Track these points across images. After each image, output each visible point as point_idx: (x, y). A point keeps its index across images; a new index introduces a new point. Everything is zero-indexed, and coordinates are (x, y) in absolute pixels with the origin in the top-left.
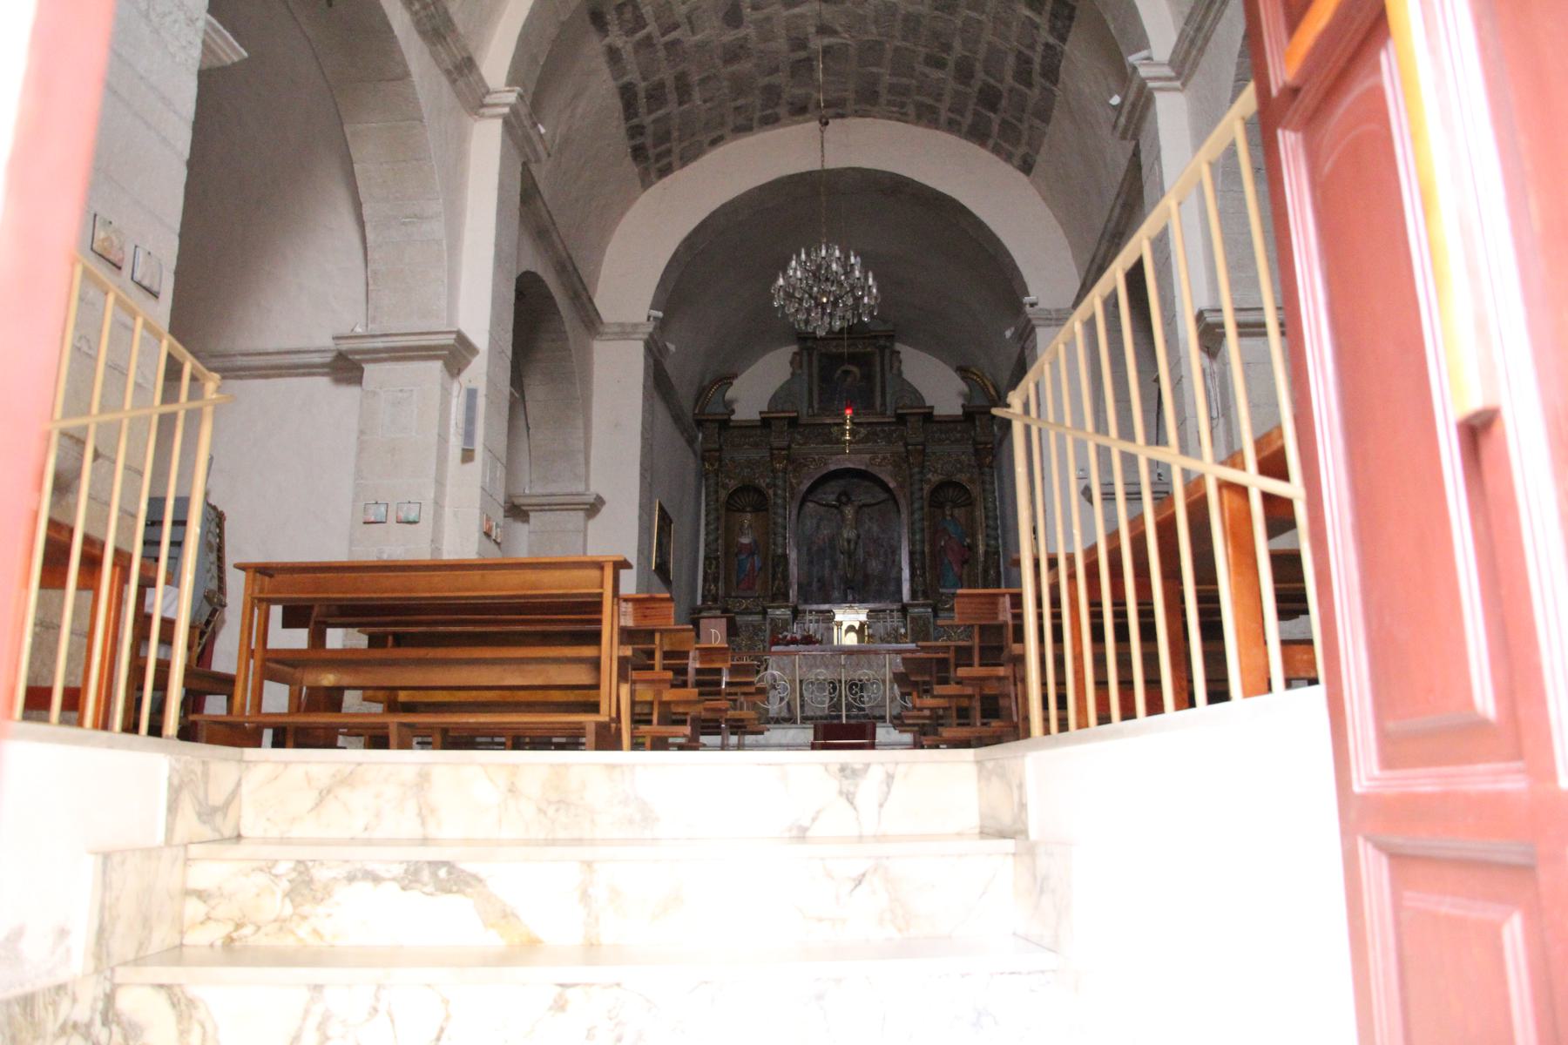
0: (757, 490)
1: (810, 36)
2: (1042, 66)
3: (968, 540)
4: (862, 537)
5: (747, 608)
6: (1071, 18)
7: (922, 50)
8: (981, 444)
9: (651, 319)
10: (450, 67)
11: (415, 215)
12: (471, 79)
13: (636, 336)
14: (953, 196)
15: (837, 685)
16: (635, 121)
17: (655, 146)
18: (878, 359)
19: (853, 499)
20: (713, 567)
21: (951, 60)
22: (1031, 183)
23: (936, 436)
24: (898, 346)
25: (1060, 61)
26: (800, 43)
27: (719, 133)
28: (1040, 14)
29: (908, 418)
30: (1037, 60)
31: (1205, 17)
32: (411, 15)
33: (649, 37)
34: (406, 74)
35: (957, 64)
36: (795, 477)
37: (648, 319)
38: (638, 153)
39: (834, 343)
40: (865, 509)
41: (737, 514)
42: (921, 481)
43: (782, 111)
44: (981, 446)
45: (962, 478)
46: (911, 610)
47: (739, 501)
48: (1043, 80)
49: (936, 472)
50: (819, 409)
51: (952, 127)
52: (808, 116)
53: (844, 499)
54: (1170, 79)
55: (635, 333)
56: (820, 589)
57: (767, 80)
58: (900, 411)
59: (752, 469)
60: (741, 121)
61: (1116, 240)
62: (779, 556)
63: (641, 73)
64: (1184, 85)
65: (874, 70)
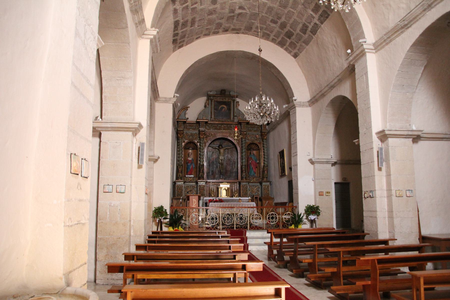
0: (194, 143)
1: (236, 9)
2: (311, 29)
3: (258, 161)
4: (225, 158)
5: (191, 181)
6: (327, 17)
7: (271, 18)
8: (263, 132)
9: (175, 97)
10: (137, 22)
11: (122, 77)
12: (142, 26)
13: (170, 102)
14: (272, 63)
15: (233, 218)
16: (176, 32)
17: (180, 39)
18: (232, 103)
19: (223, 146)
20: (181, 168)
21: (279, 22)
22: (296, 61)
23: (250, 129)
24: (238, 100)
25: (318, 29)
26: (232, 11)
27: (200, 36)
28: (316, 14)
29: (242, 123)
30: (310, 27)
31: (392, 35)
32: (129, 4)
33: (187, 6)
34: (127, 27)
35: (281, 23)
36: (206, 140)
37: (174, 97)
38: (174, 41)
39: (219, 98)
40: (226, 150)
41: (188, 150)
42: (245, 143)
43: (220, 30)
44: (264, 133)
45: (256, 142)
46: (242, 183)
48: (310, 33)
49: (249, 140)
50: (214, 118)
51: (273, 41)
52: (228, 32)
53: (221, 147)
54: (372, 49)
55: (169, 101)
56: (212, 174)
57: (218, 21)
58: (240, 121)
59: (193, 137)
60: (207, 32)
61: (332, 88)
62: (201, 165)
63: (182, 17)
64: (376, 52)
65: (253, 21)
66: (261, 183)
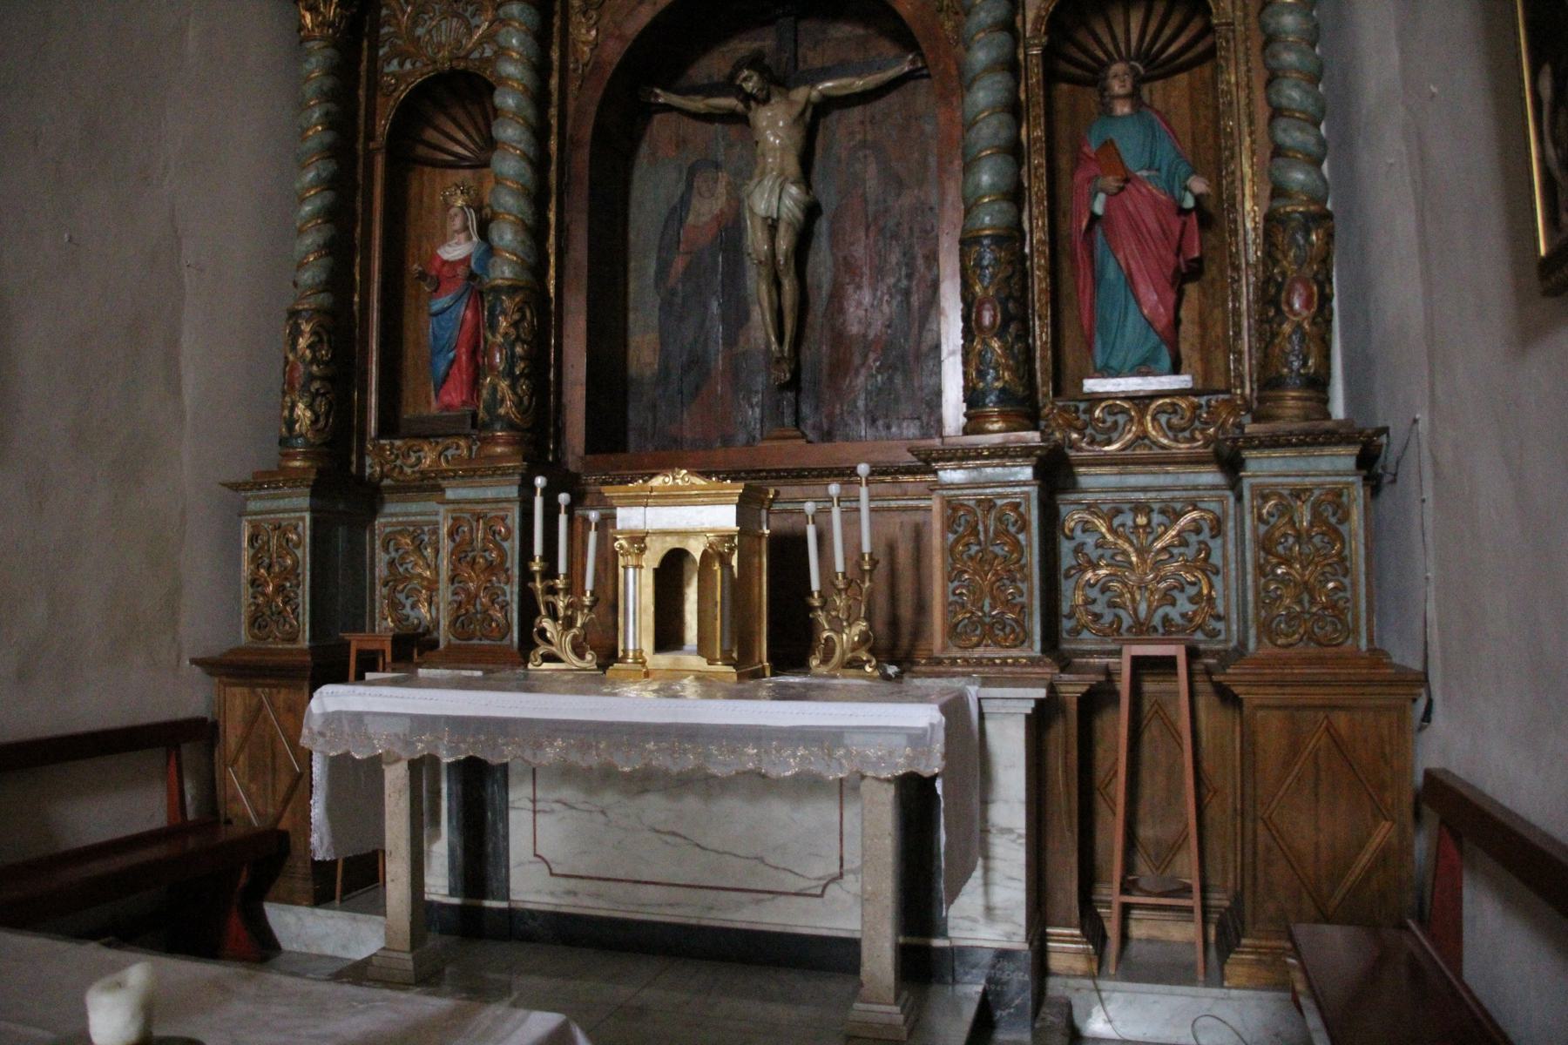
3: (1199, 185)
47: (461, 136)
66: (1231, 464)
